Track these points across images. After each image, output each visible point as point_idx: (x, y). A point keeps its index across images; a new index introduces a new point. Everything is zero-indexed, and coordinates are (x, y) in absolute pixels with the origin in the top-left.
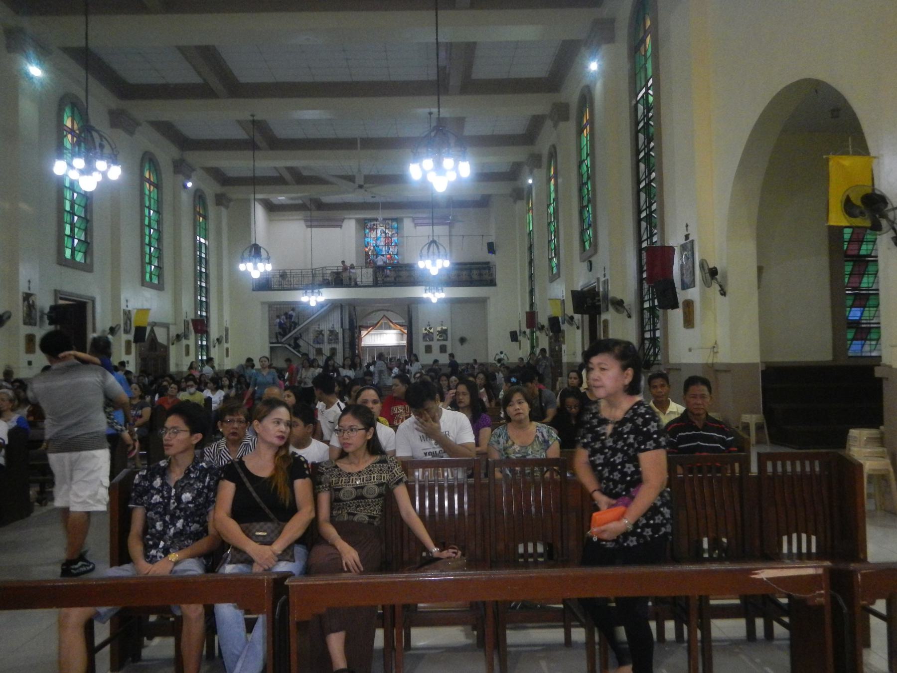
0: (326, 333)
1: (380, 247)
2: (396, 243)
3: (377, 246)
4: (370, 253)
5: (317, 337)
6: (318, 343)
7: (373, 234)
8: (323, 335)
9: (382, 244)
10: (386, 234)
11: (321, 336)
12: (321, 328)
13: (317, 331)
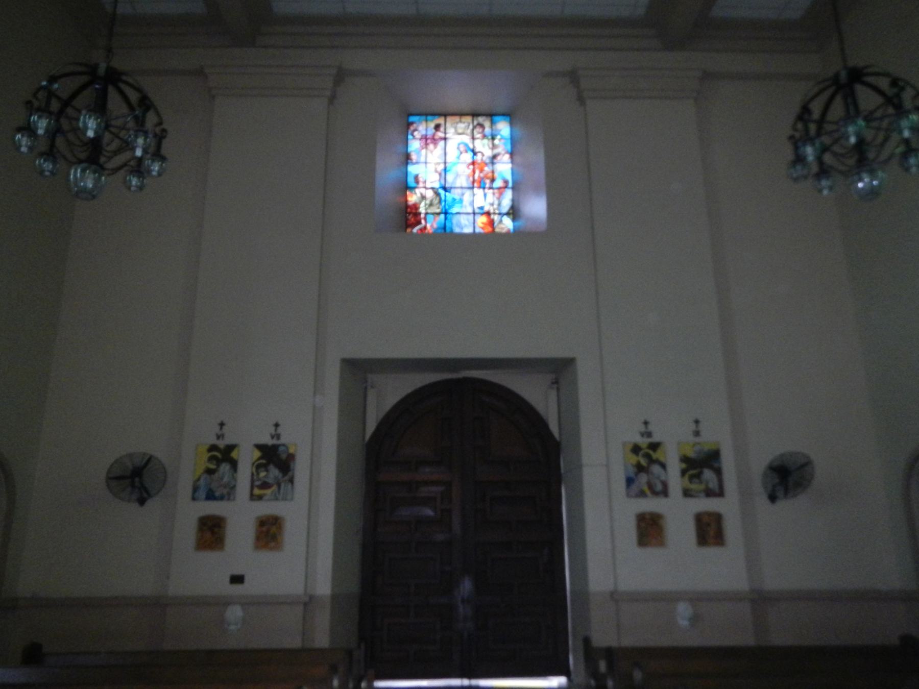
0: (247, 457)
1: (455, 194)
2: (506, 182)
3: (445, 189)
4: (422, 210)
5: (209, 472)
6: (211, 496)
7: (434, 154)
8: (234, 464)
9: (463, 181)
10: (475, 154)
11: (225, 468)
12: (228, 440)
13: (213, 448)
